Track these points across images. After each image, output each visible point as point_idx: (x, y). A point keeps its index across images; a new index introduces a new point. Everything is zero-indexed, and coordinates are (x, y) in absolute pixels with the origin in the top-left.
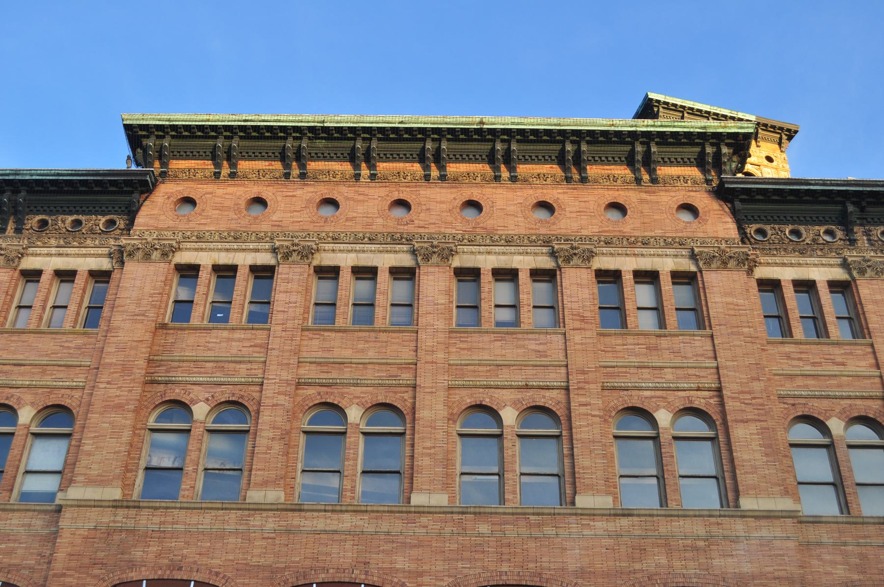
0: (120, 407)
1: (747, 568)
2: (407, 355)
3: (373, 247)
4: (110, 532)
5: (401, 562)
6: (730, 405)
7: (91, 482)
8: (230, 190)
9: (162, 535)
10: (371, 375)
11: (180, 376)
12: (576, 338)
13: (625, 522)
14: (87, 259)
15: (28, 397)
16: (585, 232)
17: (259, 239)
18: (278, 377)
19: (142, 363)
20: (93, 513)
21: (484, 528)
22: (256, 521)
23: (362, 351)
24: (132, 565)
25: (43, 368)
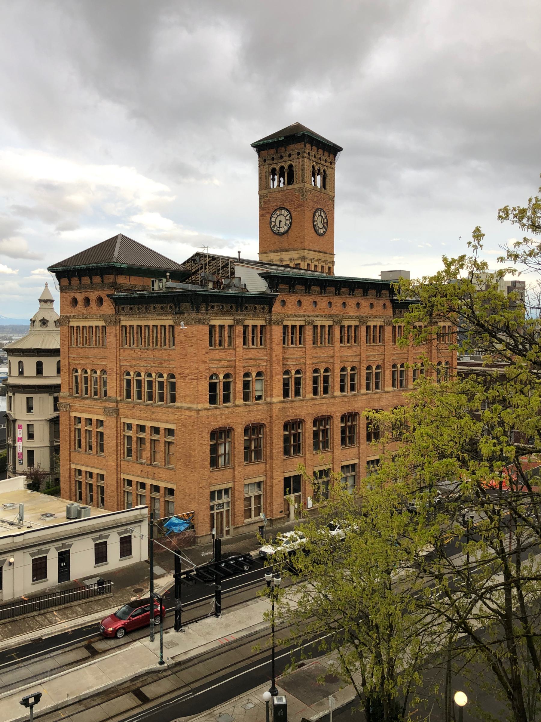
0: (279, 374)
1: (385, 404)
2: (332, 355)
3: (325, 319)
4: (282, 408)
5: (333, 409)
6: (386, 365)
7: (276, 396)
8: (293, 297)
9: (292, 408)
10: (326, 360)
11: (289, 363)
12: (362, 347)
13: (368, 396)
14: (259, 322)
15: (253, 369)
16: (366, 314)
17: (301, 317)
18: (309, 362)
19: (281, 360)
20: (278, 404)
21: (346, 400)
22: (309, 403)
23: (323, 353)
24: (288, 416)
25: (256, 360)
